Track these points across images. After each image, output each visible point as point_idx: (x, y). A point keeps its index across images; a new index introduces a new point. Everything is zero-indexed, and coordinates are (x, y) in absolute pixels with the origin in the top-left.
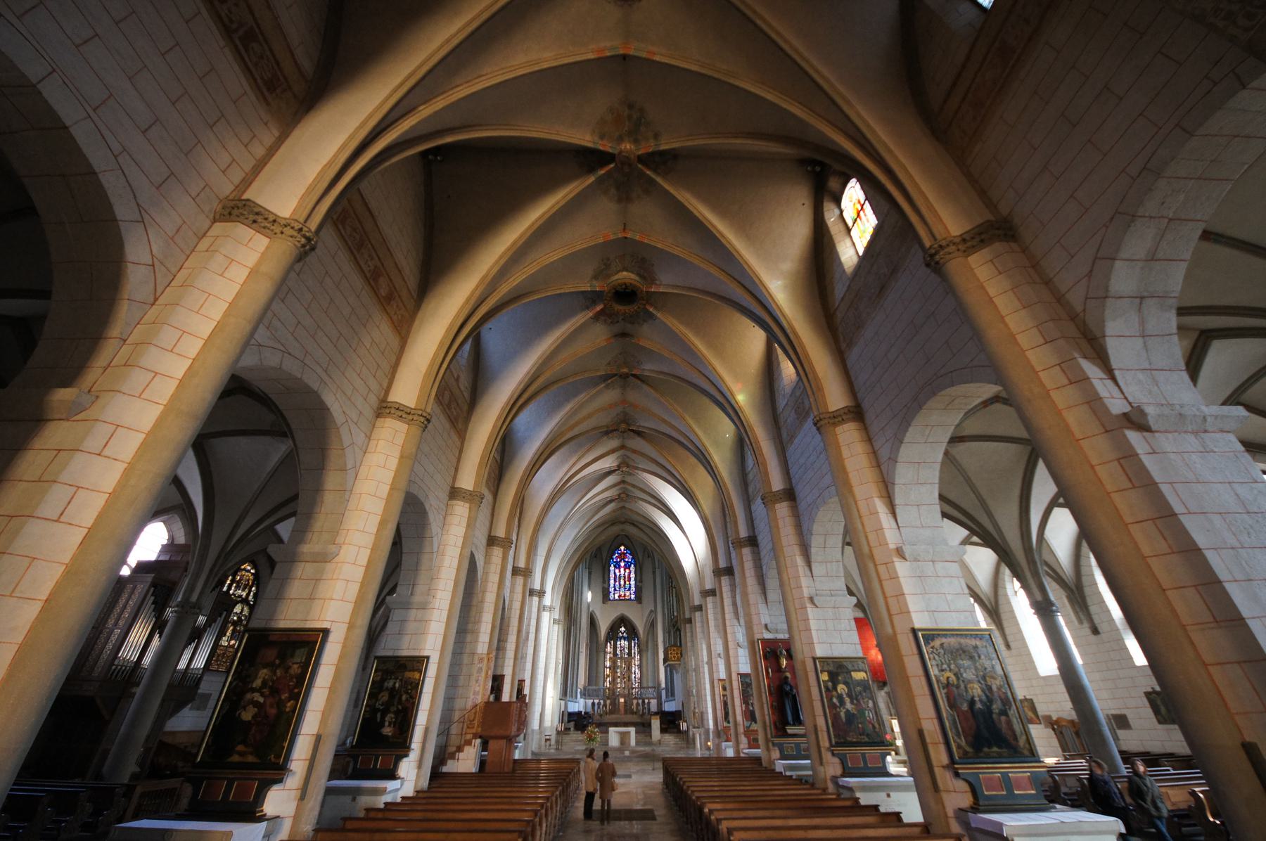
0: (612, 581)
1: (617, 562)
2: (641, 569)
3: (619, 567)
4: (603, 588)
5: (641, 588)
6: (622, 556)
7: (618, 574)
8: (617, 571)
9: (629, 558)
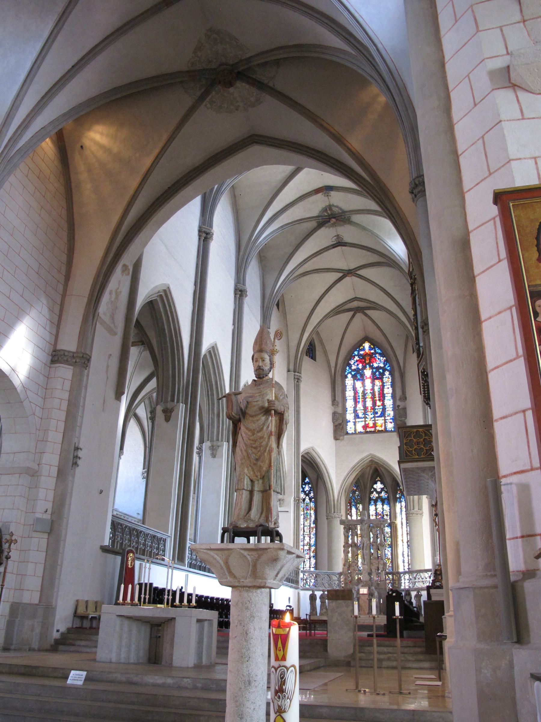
0: (350, 404)
1: (357, 370)
2: (402, 376)
3: (362, 378)
4: (334, 414)
5: (405, 409)
6: (367, 359)
7: (360, 390)
8: (359, 384)
9: (379, 362)
